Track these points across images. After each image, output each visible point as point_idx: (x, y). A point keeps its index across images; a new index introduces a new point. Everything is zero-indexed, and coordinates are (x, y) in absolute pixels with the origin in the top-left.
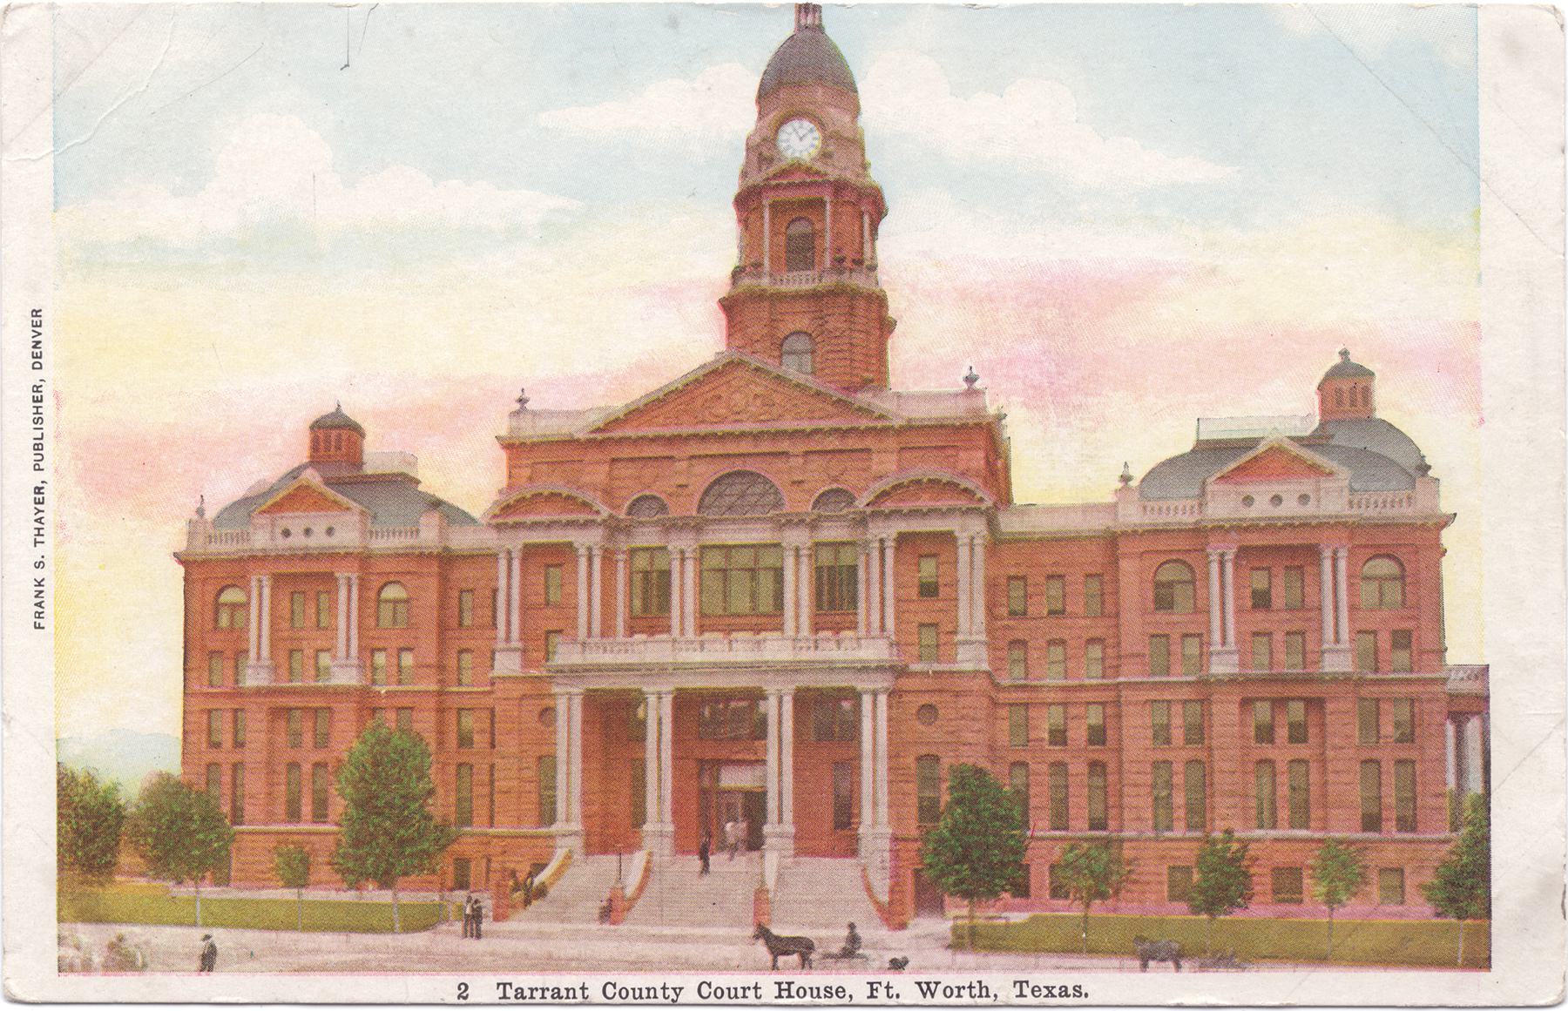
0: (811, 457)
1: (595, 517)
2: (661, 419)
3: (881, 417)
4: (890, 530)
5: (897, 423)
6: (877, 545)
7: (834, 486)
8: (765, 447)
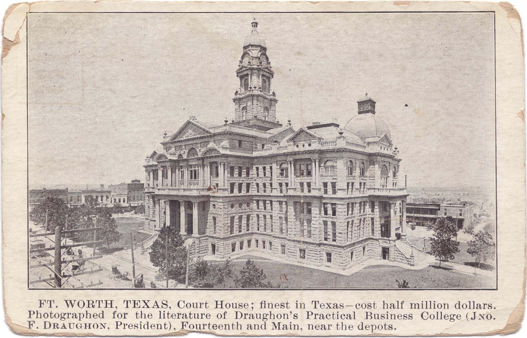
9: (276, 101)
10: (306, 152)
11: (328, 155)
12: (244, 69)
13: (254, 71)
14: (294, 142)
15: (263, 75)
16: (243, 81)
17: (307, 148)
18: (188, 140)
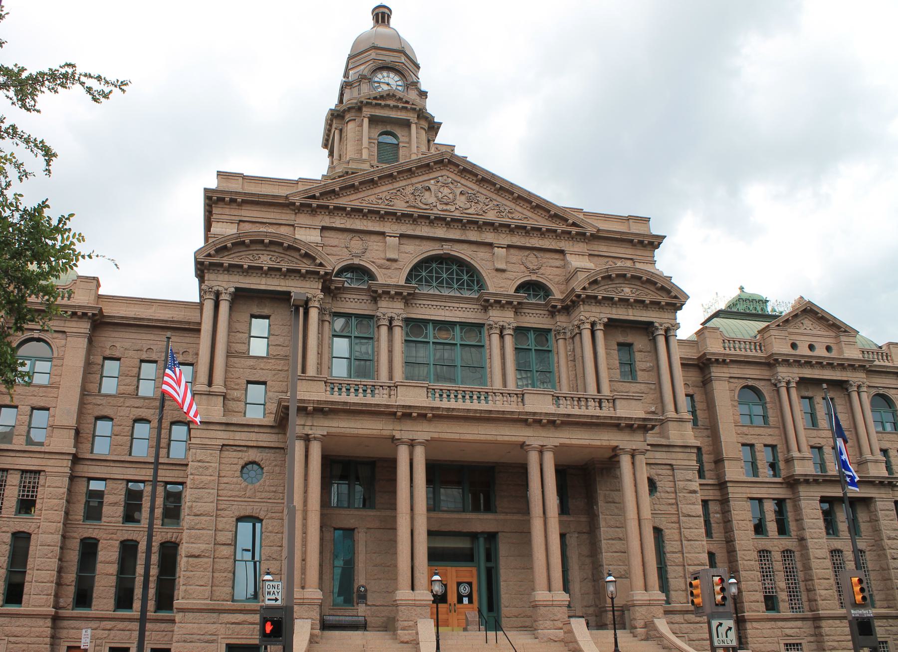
0: (512, 251)
1: (317, 269)
2: (372, 198)
3: (574, 224)
4: (603, 314)
5: (590, 231)
6: (589, 326)
7: (534, 278)
8: (473, 235)
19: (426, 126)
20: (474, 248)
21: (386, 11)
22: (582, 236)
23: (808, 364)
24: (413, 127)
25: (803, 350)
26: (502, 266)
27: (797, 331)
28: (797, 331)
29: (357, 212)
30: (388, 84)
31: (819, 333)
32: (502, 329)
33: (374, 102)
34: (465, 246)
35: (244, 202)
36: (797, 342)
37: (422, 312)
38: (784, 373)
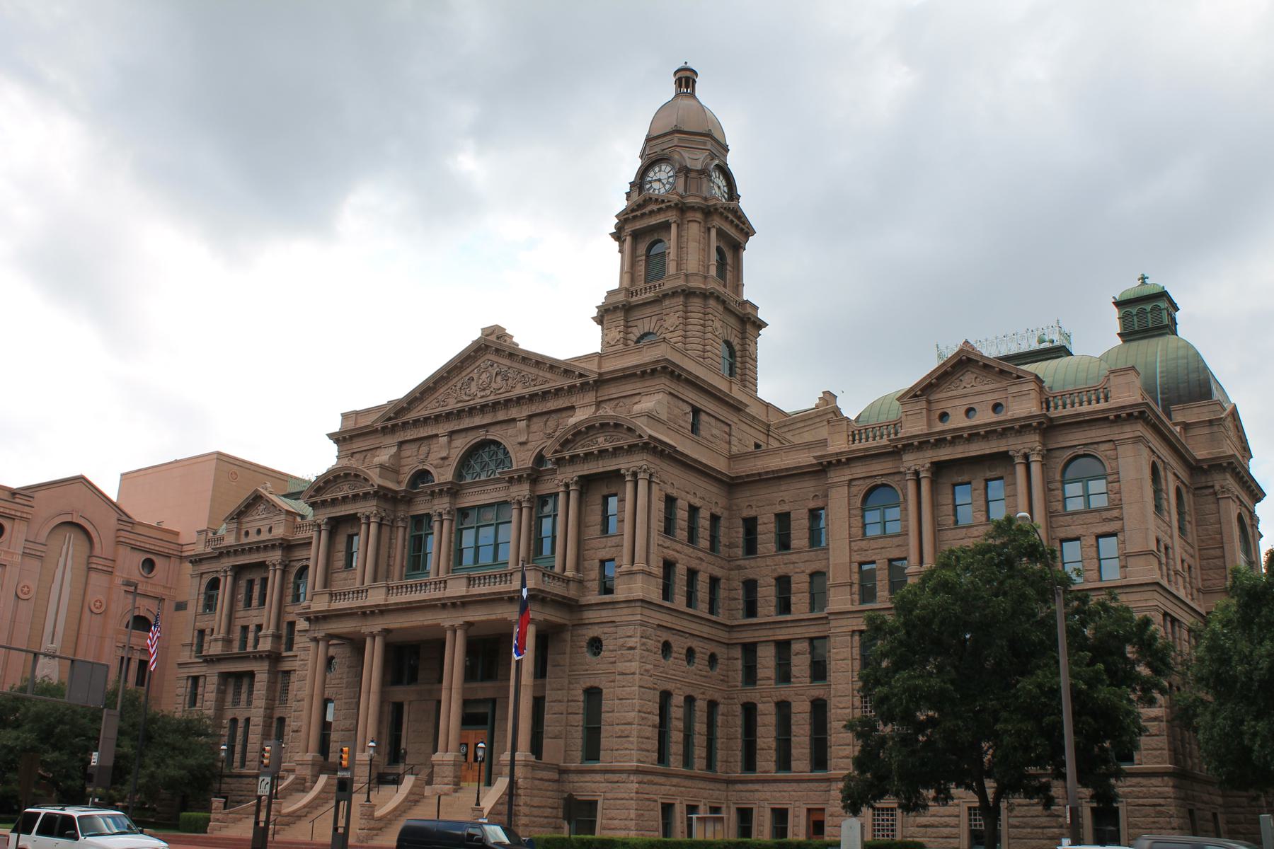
0: (535, 420)
3: (581, 375)
4: (572, 473)
8: (501, 416)
9: (760, 325)
10: (991, 433)
11: (1076, 438)
12: (655, 207)
13: (690, 215)
14: (929, 402)
15: (721, 234)
16: (642, 249)
17: (985, 417)
18: (471, 411)
19: (699, 216)
20: (504, 427)
21: (688, 74)
22: (585, 387)
23: (940, 442)
24: (674, 227)
25: (958, 421)
26: (523, 439)
27: (950, 394)
28: (950, 394)
29: (416, 423)
30: (659, 180)
31: (986, 387)
32: (519, 503)
33: (638, 213)
34: (498, 427)
35: (352, 438)
36: (949, 411)
37: (467, 501)
38: (912, 461)
